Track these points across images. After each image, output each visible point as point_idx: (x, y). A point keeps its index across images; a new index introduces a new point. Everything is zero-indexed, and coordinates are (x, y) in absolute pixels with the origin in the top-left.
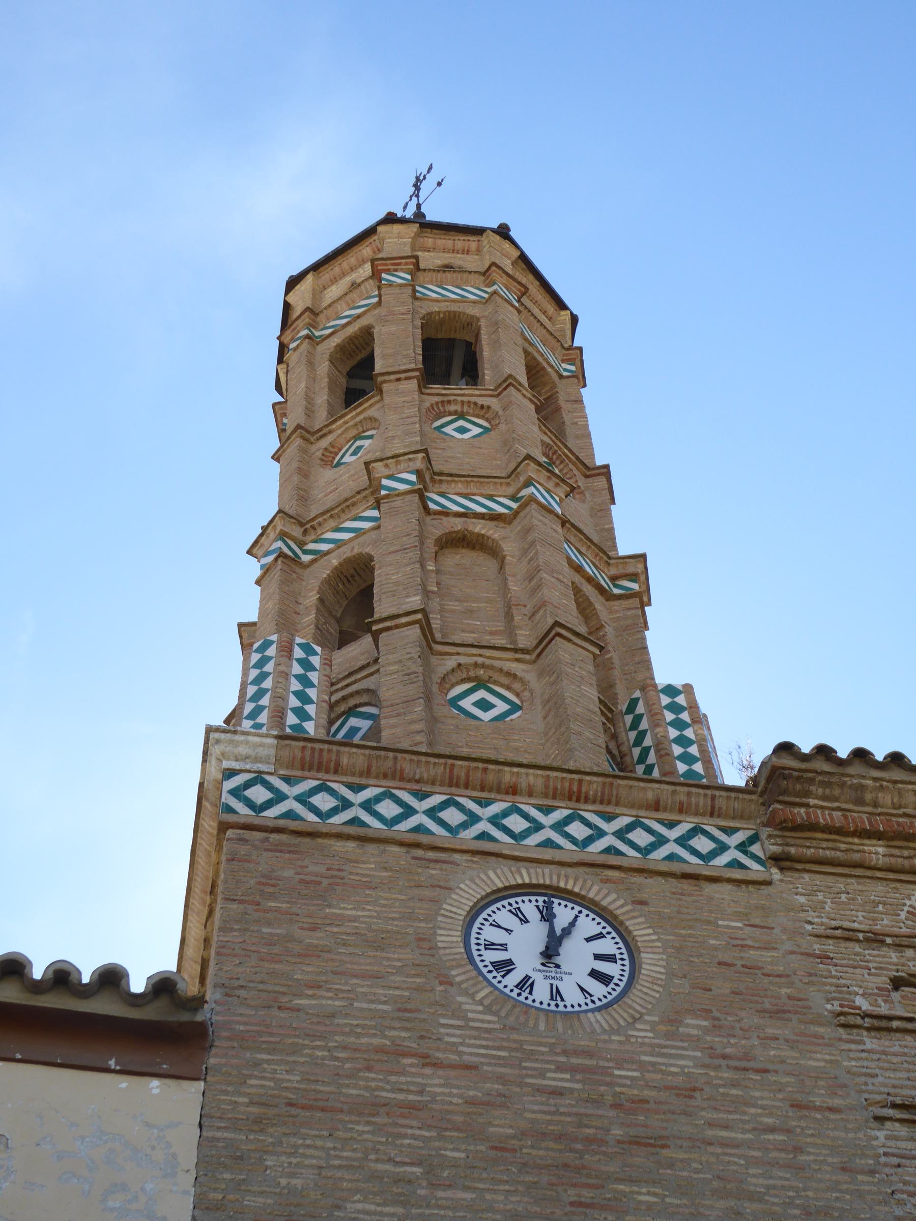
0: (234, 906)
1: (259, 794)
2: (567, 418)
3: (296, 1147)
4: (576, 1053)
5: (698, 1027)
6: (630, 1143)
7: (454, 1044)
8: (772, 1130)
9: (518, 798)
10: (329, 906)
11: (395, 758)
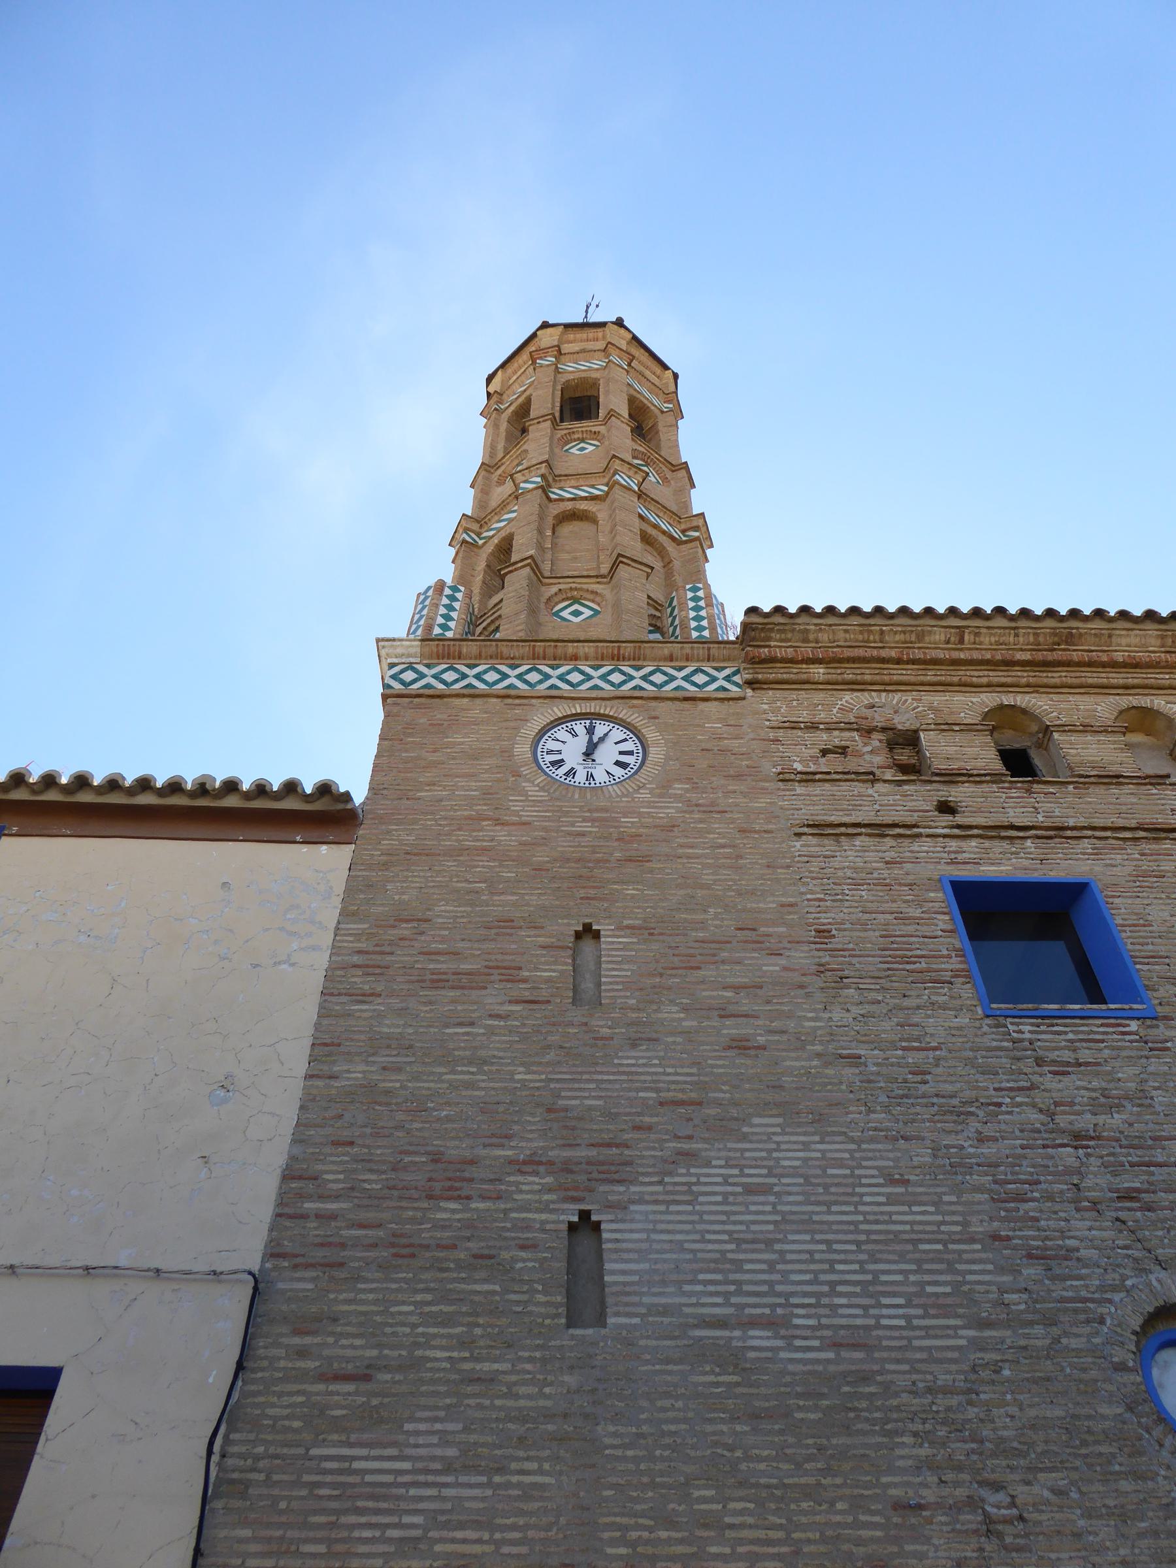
0: (386, 743)
1: (409, 676)
2: (663, 437)
3: (407, 877)
4: (597, 810)
5: (681, 789)
6: (625, 860)
7: (518, 811)
8: (723, 846)
9: (577, 662)
10: (447, 737)
11: (497, 645)
